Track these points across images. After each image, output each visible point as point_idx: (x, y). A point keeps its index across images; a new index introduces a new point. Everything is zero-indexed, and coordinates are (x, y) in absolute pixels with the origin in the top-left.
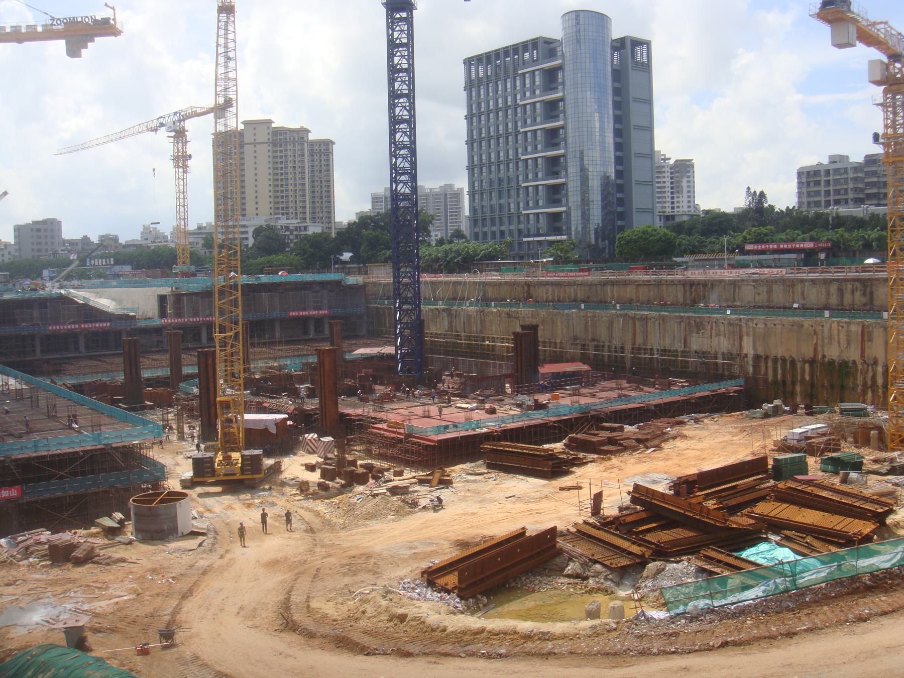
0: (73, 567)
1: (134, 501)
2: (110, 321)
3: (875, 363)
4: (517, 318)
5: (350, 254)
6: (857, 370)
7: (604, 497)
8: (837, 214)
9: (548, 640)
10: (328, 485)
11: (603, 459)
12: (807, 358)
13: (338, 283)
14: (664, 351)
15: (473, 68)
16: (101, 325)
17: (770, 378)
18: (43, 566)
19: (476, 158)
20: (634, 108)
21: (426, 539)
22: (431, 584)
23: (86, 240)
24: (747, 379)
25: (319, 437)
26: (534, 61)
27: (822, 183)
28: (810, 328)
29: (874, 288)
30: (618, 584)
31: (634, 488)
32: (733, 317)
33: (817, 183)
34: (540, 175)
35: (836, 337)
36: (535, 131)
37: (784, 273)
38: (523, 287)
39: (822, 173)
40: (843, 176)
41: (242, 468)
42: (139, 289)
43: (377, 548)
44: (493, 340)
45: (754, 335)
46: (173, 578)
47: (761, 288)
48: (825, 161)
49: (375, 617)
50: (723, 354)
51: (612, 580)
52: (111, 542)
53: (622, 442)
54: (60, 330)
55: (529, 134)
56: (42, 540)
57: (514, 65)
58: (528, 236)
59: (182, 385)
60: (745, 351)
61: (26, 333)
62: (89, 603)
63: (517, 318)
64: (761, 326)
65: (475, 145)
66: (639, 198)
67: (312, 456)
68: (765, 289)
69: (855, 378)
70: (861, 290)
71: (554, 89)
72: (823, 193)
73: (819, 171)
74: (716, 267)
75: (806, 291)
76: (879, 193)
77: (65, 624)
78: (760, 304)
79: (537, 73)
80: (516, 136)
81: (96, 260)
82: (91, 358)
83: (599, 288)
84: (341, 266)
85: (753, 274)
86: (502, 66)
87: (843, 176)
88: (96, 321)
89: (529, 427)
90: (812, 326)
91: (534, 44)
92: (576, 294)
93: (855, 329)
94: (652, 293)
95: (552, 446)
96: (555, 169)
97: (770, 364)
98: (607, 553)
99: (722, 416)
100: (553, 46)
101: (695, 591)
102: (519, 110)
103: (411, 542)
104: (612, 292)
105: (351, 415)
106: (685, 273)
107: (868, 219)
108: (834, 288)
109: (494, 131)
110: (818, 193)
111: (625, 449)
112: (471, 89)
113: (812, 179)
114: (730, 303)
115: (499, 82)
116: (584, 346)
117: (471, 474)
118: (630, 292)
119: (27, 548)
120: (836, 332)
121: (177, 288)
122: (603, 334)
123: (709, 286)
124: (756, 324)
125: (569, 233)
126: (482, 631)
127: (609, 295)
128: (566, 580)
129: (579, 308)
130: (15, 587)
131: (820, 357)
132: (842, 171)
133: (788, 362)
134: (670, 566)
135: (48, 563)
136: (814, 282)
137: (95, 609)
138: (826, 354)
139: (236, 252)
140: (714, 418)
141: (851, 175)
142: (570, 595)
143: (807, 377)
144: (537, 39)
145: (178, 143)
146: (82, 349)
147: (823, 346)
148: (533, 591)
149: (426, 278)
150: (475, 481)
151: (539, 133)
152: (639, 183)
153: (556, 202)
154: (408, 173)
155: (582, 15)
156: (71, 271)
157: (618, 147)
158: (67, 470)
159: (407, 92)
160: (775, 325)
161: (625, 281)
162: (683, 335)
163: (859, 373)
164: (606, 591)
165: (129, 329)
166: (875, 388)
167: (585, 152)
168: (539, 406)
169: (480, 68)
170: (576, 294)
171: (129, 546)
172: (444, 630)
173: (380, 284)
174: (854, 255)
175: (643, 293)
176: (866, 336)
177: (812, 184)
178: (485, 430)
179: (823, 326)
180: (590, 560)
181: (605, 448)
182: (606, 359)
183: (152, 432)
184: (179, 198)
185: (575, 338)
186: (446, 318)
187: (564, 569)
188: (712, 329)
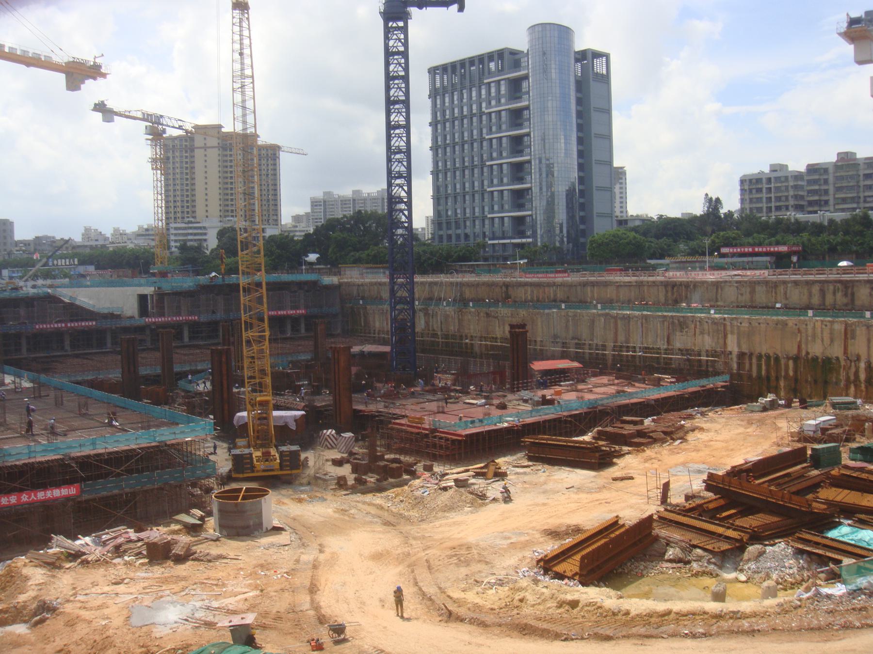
0: (175, 564)
1: (215, 496)
2: (96, 320)
3: (858, 358)
4: (496, 317)
5: (318, 256)
6: (840, 367)
7: (671, 486)
8: (796, 220)
9: (740, 618)
10: (366, 479)
11: (638, 451)
12: (791, 355)
13: (315, 283)
14: (646, 349)
15: (438, 77)
16: (87, 324)
17: (754, 373)
18: (142, 564)
19: (440, 164)
20: (595, 117)
21: (514, 529)
22: (546, 571)
23: (54, 237)
24: (732, 375)
25: (339, 432)
27: (764, 190)
28: (794, 326)
29: (855, 289)
30: (721, 567)
31: (708, 477)
32: (717, 316)
33: (759, 190)
34: (505, 180)
35: (820, 335)
36: (501, 138)
37: (766, 274)
38: (501, 287)
39: (764, 181)
40: (784, 184)
41: (281, 464)
42: (118, 289)
43: (471, 539)
44: (472, 338)
45: (739, 334)
46: (287, 573)
47: (744, 289)
48: (767, 170)
49: (539, 604)
50: (707, 351)
51: (715, 564)
52: (196, 539)
53: (651, 434)
54: (47, 328)
55: (494, 141)
56: (132, 538)
57: (479, 73)
58: (493, 239)
59: (182, 383)
60: (729, 349)
61: (13, 332)
62: (216, 599)
63: (496, 317)
64: (745, 324)
65: (440, 151)
66: (598, 205)
67: (332, 451)
68: (748, 290)
69: (838, 373)
70: (842, 291)
71: (519, 98)
72: (764, 200)
73: (761, 179)
74: (698, 269)
75: (788, 292)
76: (820, 200)
77: (231, 621)
78: (743, 304)
79: (502, 82)
80: (482, 142)
81: (59, 260)
82: (77, 356)
83: (579, 288)
84: (308, 267)
85: (736, 275)
87: (784, 184)
88: (82, 320)
89: (545, 422)
90: (796, 325)
91: (500, 54)
92: (555, 295)
93: (839, 327)
94: (633, 293)
95: (580, 438)
96: (521, 175)
97: (754, 361)
98: (703, 539)
99: (723, 410)
100: (517, 57)
101: (799, 571)
102: (484, 117)
103: (502, 533)
104: (592, 292)
105: (364, 411)
106: (667, 275)
107: (826, 224)
108: (816, 289)
109: (459, 137)
110: (759, 200)
111: (655, 441)
112: (435, 97)
113: (754, 187)
114: (712, 303)
115: (464, 91)
116: (564, 345)
117: (518, 467)
118: (610, 292)
119: (117, 548)
120: (820, 330)
121: (159, 288)
122: (584, 333)
123: (692, 287)
124: (741, 323)
125: (534, 235)
126: (669, 613)
127: (589, 295)
128: (669, 565)
129: (559, 308)
130: (126, 586)
131: (804, 353)
132: (783, 179)
133: (772, 359)
134: (769, 549)
135: (147, 560)
136: (796, 283)
137: (226, 605)
138: (810, 351)
139: (258, 252)
140: (717, 412)
141: (791, 183)
142: (679, 579)
143: (791, 373)
144: (503, 50)
145: (156, 145)
146: (67, 347)
147: (807, 344)
148: (642, 576)
149: (418, 279)
150: (525, 473)
151: (504, 140)
152: (600, 189)
153: (520, 207)
154: (404, 177)
155: (548, 27)
156: (37, 271)
157: (581, 154)
158: (123, 468)
159: (404, 98)
160: (759, 324)
161: (606, 282)
162: (666, 334)
163: (842, 370)
164: (711, 574)
165: (114, 328)
166: (858, 383)
168: (545, 401)
170: (555, 295)
171: (218, 542)
172: (627, 613)
173: (354, 285)
174: (824, 258)
175: (624, 294)
176: (848, 334)
177: (754, 191)
178: (506, 425)
179: (806, 325)
180: (690, 545)
181: (636, 440)
182: (587, 356)
183: (204, 429)
184: (157, 200)
185: (555, 336)
186: (423, 317)
187: (664, 554)
188: (695, 327)
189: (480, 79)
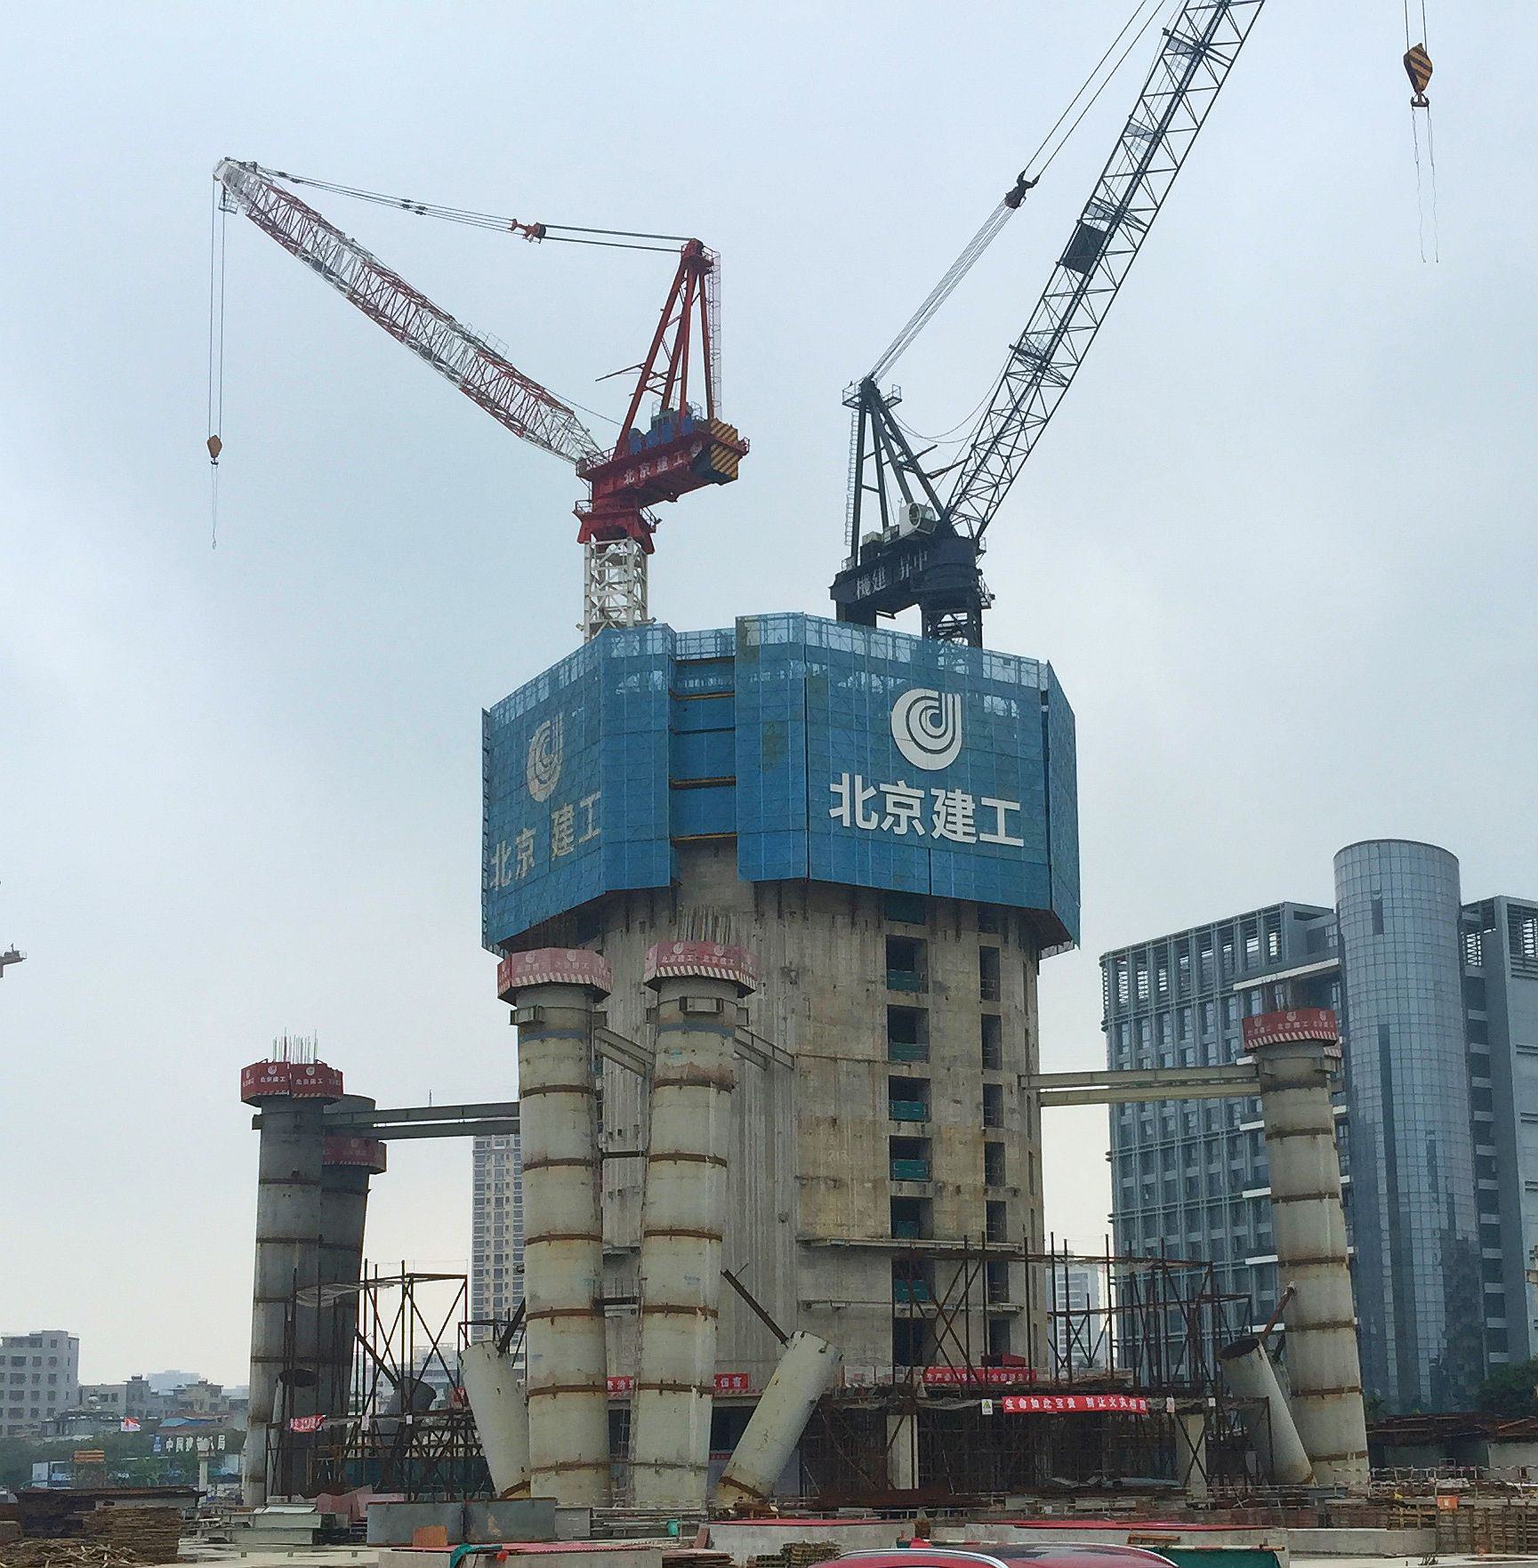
26: (1269, 959)
57: (1222, 965)
86: (1194, 972)
91: (1272, 918)
112: (1119, 1027)
144: (1276, 908)
167: (1393, 1029)
169: (1144, 977)
189: (1226, 983)
